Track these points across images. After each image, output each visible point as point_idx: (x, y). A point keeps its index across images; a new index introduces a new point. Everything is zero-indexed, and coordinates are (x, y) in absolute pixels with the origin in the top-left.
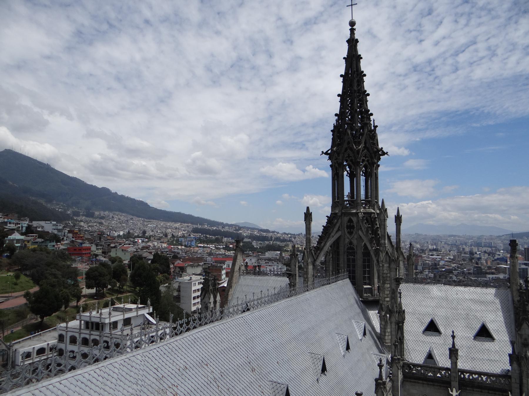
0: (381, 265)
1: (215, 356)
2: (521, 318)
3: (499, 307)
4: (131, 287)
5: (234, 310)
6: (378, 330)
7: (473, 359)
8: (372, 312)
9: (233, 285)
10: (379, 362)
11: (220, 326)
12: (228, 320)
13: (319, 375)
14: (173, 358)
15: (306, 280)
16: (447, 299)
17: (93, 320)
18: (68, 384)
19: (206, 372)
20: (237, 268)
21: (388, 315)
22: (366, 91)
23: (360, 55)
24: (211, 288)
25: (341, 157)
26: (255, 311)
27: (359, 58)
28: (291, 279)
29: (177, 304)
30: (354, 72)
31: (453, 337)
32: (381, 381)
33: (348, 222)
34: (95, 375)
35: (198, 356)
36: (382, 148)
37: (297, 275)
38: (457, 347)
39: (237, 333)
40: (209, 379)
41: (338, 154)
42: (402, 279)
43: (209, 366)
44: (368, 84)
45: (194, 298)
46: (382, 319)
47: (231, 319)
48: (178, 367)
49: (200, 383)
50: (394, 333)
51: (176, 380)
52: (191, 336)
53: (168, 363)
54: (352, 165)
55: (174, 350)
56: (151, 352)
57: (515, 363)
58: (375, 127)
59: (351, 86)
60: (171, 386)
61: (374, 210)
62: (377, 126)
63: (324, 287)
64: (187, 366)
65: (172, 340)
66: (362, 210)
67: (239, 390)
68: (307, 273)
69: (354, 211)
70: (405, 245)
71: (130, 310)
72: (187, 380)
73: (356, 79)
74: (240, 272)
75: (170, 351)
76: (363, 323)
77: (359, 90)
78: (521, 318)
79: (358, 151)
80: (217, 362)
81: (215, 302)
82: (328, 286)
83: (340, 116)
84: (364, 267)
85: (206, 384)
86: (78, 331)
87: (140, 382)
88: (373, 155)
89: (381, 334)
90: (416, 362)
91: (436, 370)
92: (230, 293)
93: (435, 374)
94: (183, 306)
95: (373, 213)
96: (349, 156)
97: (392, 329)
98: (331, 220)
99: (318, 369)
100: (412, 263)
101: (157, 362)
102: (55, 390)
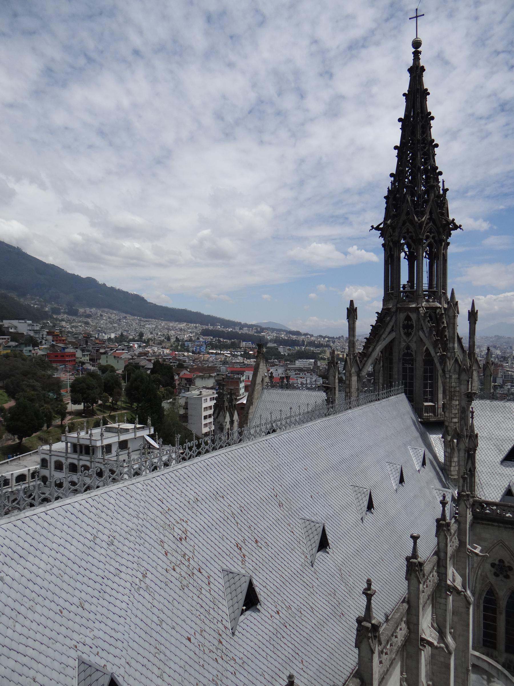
0: (448, 376)
4: (126, 403)
5: (256, 431)
6: (442, 459)
8: (434, 436)
9: (254, 400)
10: (442, 498)
11: (239, 450)
12: (249, 444)
13: (364, 513)
15: (348, 395)
17: (82, 442)
18: (55, 515)
19: (222, 505)
20: (259, 380)
21: (455, 441)
23: (427, 90)
24: (226, 404)
25: (396, 234)
26: (282, 433)
27: (426, 93)
28: (329, 393)
29: (184, 424)
30: (418, 114)
32: (444, 522)
33: (405, 320)
34: (88, 506)
36: (453, 220)
37: (337, 389)
40: (226, 514)
41: (394, 229)
42: (475, 394)
43: (225, 498)
44: (436, 131)
45: (205, 418)
46: (447, 445)
47: (253, 442)
48: (187, 499)
49: (215, 519)
50: (462, 463)
51: (186, 515)
52: (202, 462)
53: (175, 494)
54: (413, 244)
55: (182, 478)
58: (445, 190)
59: (413, 133)
60: (180, 522)
61: (440, 303)
62: (447, 190)
63: (372, 404)
64: (199, 498)
65: (180, 466)
66: (424, 304)
67: (263, 529)
68: (349, 386)
69: (414, 306)
70: (480, 351)
71: (127, 430)
72: (198, 514)
74: (263, 385)
76: (422, 450)
77: (424, 140)
80: (236, 494)
81: (232, 422)
82: (377, 402)
83: (398, 177)
84: (425, 378)
85: (222, 520)
86: (64, 455)
87: (141, 515)
88: (441, 230)
89: (445, 464)
90: (490, 500)
92: (250, 411)
94: (192, 427)
95: (440, 308)
96: (408, 232)
97: (461, 459)
98: (382, 317)
99: (362, 505)
100: (489, 374)
102: (40, 521)
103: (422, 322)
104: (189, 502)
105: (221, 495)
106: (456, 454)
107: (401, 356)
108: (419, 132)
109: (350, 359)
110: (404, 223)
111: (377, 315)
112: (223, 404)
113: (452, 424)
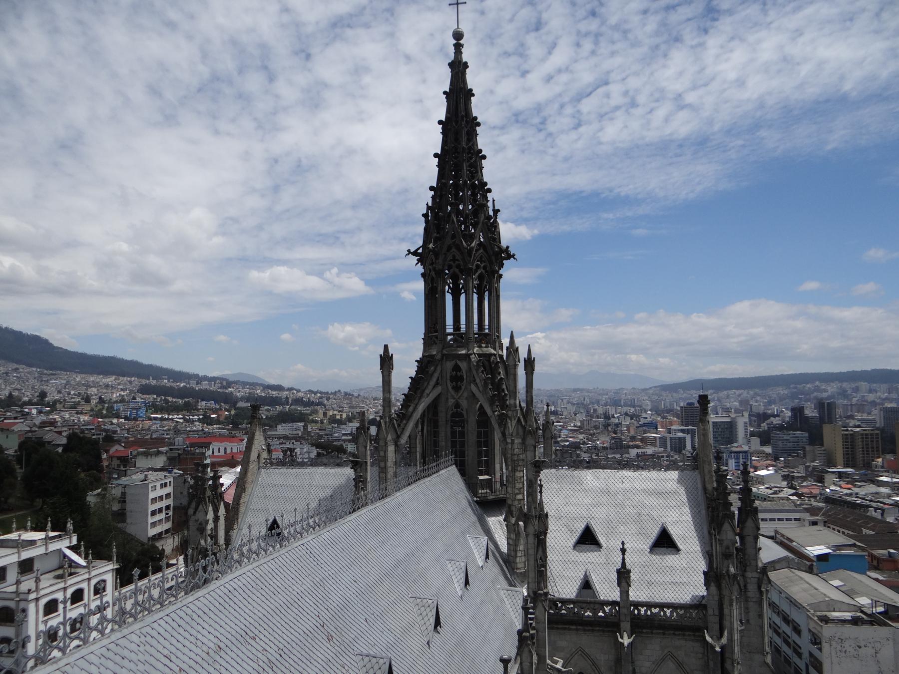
0: (509, 441)
1: (266, 620)
2: (721, 515)
3: (684, 498)
7: (650, 583)
8: (493, 518)
9: (249, 487)
11: (269, 564)
12: (281, 552)
14: (194, 632)
16: (607, 491)
19: (254, 651)
20: (254, 455)
21: (521, 523)
22: (481, 151)
23: (471, 90)
24: (209, 493)
25: (440, 261)
26: (322, 532)
30: (462, 117)
31: (623, 551)
35: (237, 622)
36: (508, 247)
37: (369, 464)
38: (628, 567)
39: (297, 575)
40: (261, 663)
41: (437, 255)
42: (543, 462)
43: (258, 640)
45: (153, 513)
46: (512, 530)
48: (205, 649)
50: (531, 552)
52: (222, 588)
53: (187, 643)
55: (195, 617)
56: (155, 625)
57: (712, 584)
59: (457, 140)
61: (495, 349)
62: (498, 211)
63: (422, 482)
64: (222, 645)
65: (191, 598)
66: (476, 350)
68: (385, 459)
69: (464, 352)
70: (539, 407)
73: (466, 130)
74: (259, 463)
75: (188, 619)
76: (484, 539)
77: (470, 148)
78: (721, 515)
79: (470, 252)
80: (271, 631)
81: (216, 519)
82: (427, 479)
83: (439, 191)
84: (479, 444)
88: (493, 258)
89: (509, 555)
90: (564, 596)
91: (597, 606)
92: (242, 501)
93: (595, 612)
95: (495, 355)
96: (454, 260)
98: (424, 365)
99: (428, 623)
101: (167, 645)
103: (474, 372)
104: (208, 653)
105: (252, 635)
106: (522, 541)
107: (449, 416)
108: (464, 138)
109: (385, 423)
110: (449, 248)
111: (416, 364)
112: (204, 494)
113: (517, 502)
